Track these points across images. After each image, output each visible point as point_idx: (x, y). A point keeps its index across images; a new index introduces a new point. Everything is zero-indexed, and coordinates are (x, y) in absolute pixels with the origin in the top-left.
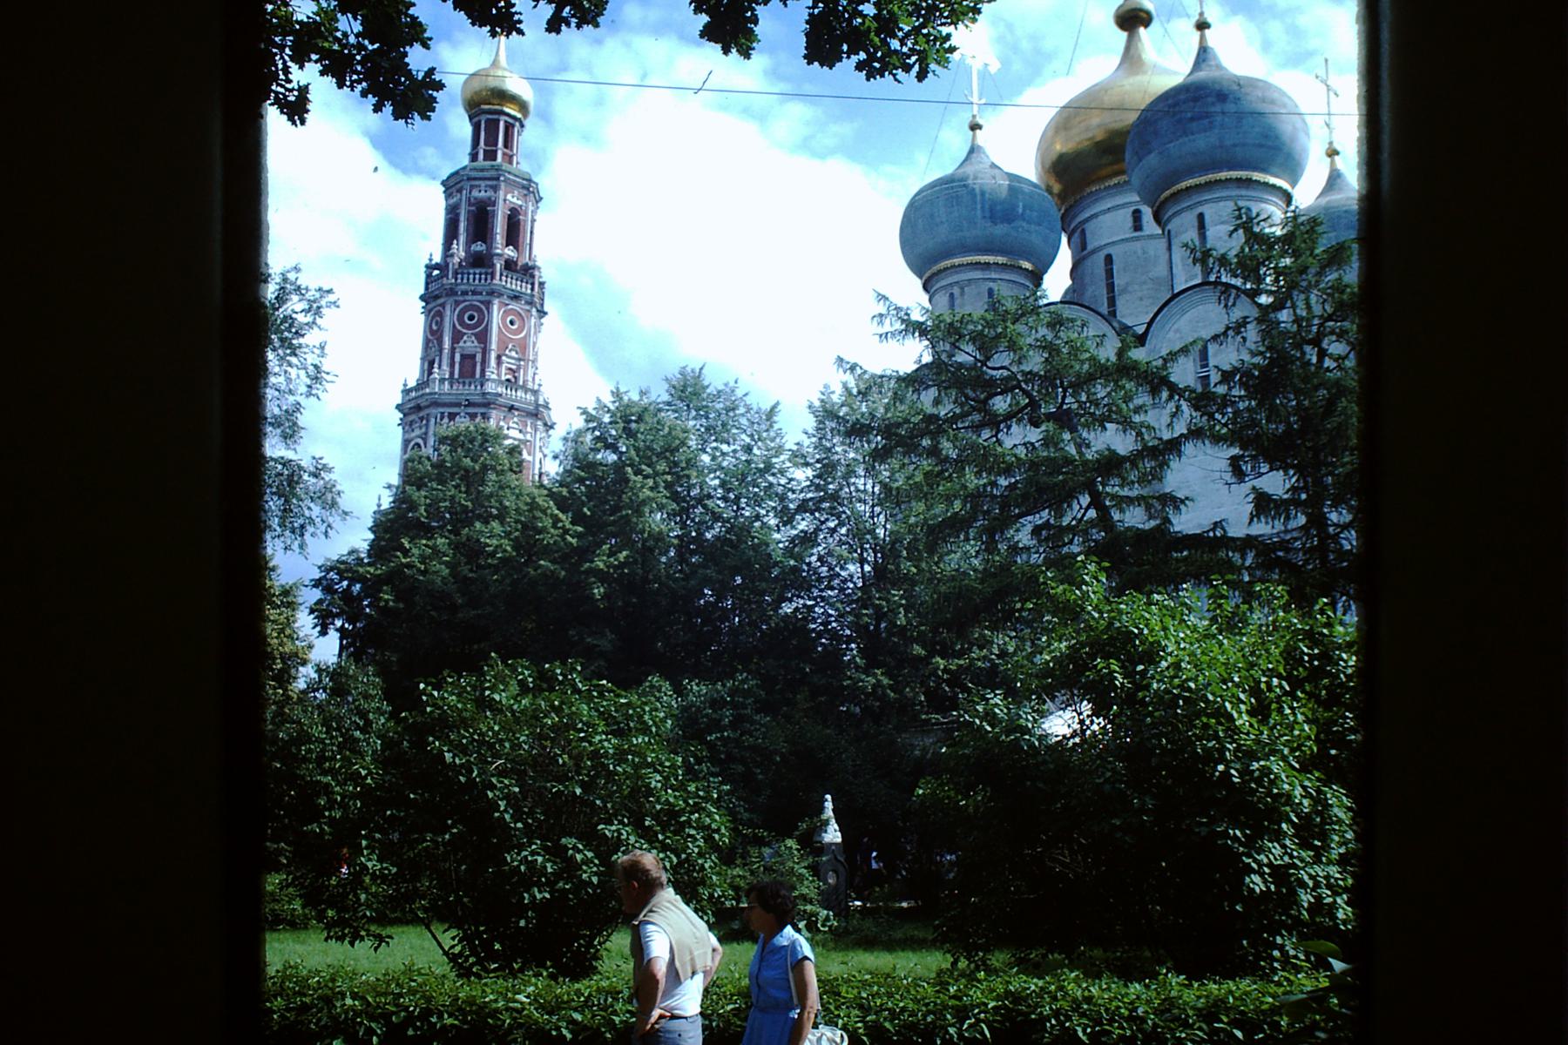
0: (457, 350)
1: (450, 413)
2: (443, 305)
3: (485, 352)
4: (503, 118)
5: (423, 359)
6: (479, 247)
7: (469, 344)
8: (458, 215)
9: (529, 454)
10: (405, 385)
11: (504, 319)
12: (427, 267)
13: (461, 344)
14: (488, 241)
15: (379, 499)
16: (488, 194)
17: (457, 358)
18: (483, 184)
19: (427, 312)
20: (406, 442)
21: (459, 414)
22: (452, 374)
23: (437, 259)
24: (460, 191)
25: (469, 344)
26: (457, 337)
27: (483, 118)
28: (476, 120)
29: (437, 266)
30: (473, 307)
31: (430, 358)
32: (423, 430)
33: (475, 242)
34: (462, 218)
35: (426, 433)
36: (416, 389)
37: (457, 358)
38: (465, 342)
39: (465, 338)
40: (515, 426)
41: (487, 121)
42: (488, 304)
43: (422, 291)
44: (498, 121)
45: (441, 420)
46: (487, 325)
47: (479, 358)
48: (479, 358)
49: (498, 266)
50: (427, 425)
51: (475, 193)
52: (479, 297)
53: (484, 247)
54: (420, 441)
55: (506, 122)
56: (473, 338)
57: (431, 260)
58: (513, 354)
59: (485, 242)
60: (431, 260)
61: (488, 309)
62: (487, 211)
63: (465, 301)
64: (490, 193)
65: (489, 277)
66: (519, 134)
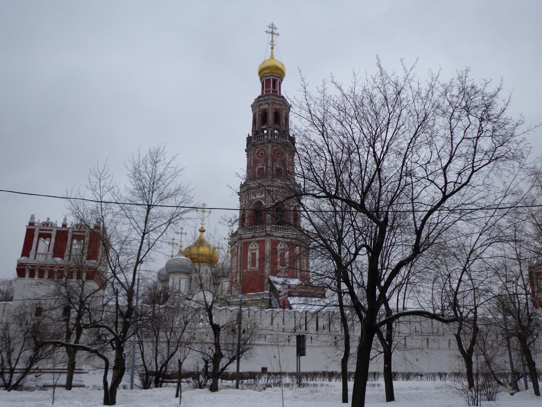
4: (271, 78)
23: (251, 135)
27: (264, 79)
28: (262, 81)
41: (266, 80)
43: (246, 148)
44: (270, 79)
55: (273, 79)
60: (249, 136)
61: (267, 149)
64: (267, 106)
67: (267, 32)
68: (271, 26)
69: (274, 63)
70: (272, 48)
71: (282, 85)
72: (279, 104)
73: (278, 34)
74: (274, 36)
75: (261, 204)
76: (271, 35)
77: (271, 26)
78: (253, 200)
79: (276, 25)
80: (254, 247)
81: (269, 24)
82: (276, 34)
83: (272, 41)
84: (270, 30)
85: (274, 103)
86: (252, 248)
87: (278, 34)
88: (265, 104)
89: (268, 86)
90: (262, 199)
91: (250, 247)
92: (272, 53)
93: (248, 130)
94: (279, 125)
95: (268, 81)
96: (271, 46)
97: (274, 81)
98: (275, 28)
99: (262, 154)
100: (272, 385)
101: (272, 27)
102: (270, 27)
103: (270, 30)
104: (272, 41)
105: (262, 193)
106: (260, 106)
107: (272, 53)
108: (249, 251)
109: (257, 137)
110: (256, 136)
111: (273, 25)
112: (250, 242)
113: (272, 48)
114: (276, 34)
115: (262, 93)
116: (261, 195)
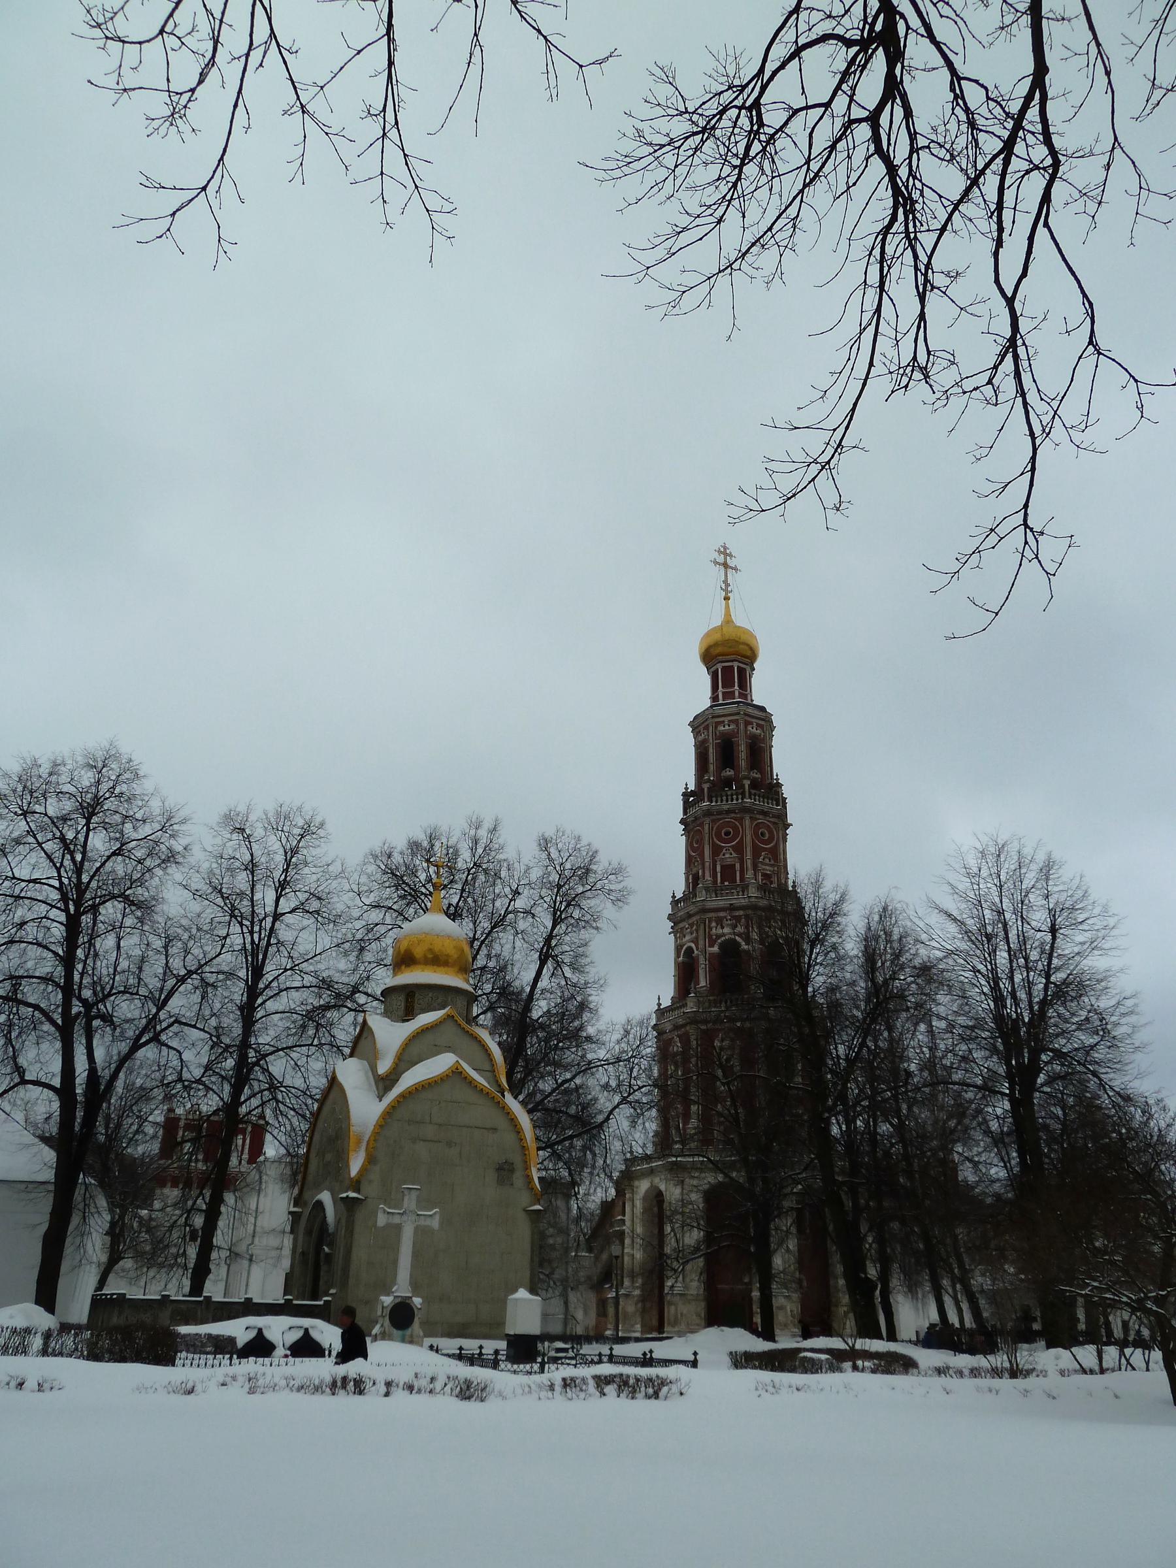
2: (702, 825)
3: (742, 861)
4: (736, 664)
5: (687, 874)
6: (729, 773)
7: (729, 856)
8: (707, 749)
10: (674, 897)
11: (756, 833)
12: (684, 794)
13: (721, 856)
15: (659, 999)
17: (718, 869)
18: (726, 719)
19: (687, 831)
20: (678, 949)
21: (725, 917)
22: (715, 882)
23: (692, 787)
24: (706, 728)
25: (727, 856)
26: (716, 851)
27: (719, 667)
29: (692, 793)
30: (728, 824)
31: (694, 870)
32: (694, 935)
34: (711, 750)
35: (697, 938)
36: (685, 898)
37: (718, 869)
39: (724, 851)
41: (724, 668)
42: (741, 820)
47: (738, 866)
48: (738, 866)
49: (747, 787)
50: (697, 931)
52: (733, 815)
53: (732, 773)
54: (693, 945)
55: (738, 667)
56: (731, 851)
57: (686, 788)
58: (767, 861)
60: (686, 788)
62: (732, 742)
63: (721, 819)
65: (740, 797)
66: (750, 677)
67: (716, 563)
68: (722, 550)
69: (729, 633)
70: (727, 598)
71: (753, 680)
72: (758, 725)
73: (735, 569)
74: (729, 571)
75: (739, 945)
76: (722, 568)
77: (722, 550)
78: (718, 937)
79: (732, 549)
81: (718, 545)
82: (732, 568)
83: (725, 582)
84: (721, 559)
85: (747, 723)
87: (735, 569)
89: (728, 683)
92: (727, 607)
93: (687, 776)
94: (761, 771)
95: (728, 671)
96: (723, 594)
97: (742, 672)
98: (731, 555)
99: (727, 834)
100: (966, 1372)
101: (724, 551)
102: (720, 552)
103: (721, 559)
104: (725, 582)
105: (738, 919)
106: (718, 724)
107: (727, 607)
111: (725, 548)
113: (727, 598)
114: (732, 568)
115: (714, 698)
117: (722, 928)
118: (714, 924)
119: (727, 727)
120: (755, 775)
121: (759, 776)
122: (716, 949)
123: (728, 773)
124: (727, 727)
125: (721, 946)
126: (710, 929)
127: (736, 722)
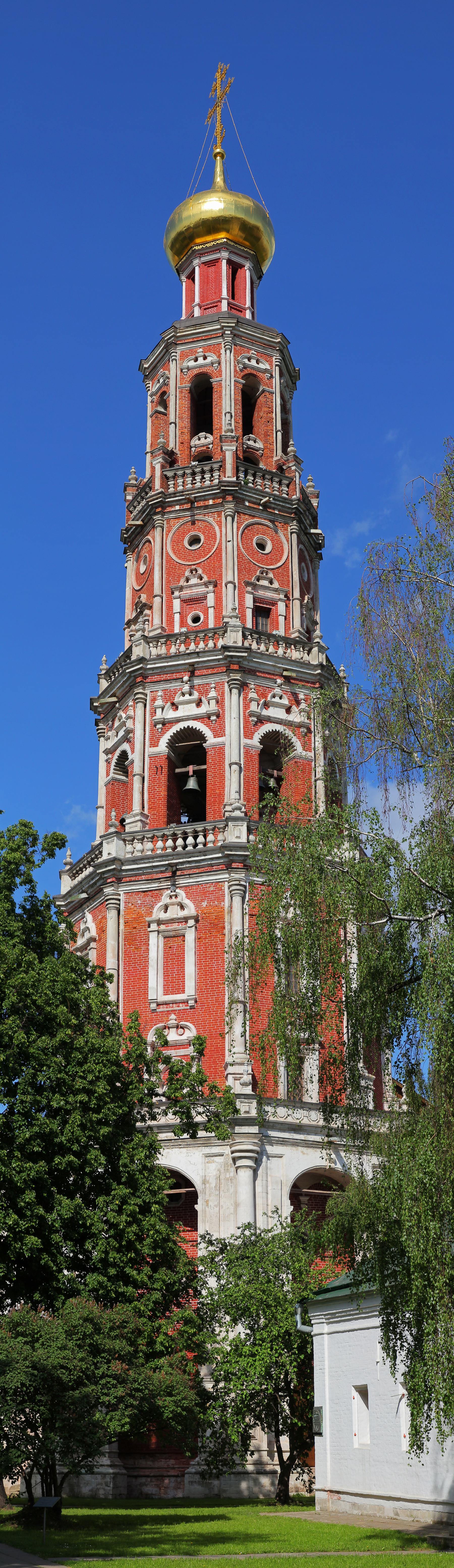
0: (177, 594)
1: (164, 690)
6: (204, 440)
9: (306, 747)
13: (182, 582)
14: (215, 432)
16: (209, 360)
17: (177, 605)
33: (195, 431)
38: (187, 580)
40: (277, 699)
45: (154, 700)
46: (219, 548)
47: (211, 600)
51: (192, 364)
53: (210, 438)
54: (126, 746)
59: (212, 434)
75: (202, 737)
80: (174, 912)
86: (163, 916)
88: (208, 349)
90: (205, 718)
91: (158, 913)
105: (204, 690)
108: (154, 927)
109: (175, 477)
110: (170, 474)
112: (156, 894)
116: (199, 703)
117: (175, 706)
118: (159, 702)
119: (201, 361)
120: (251, 443)
121: (259, 445)
122: (163, 747)
123: (203, 441)
124: (201, 361)
125: (172, 743)
126: (154, 712)
127: (216, 350)
